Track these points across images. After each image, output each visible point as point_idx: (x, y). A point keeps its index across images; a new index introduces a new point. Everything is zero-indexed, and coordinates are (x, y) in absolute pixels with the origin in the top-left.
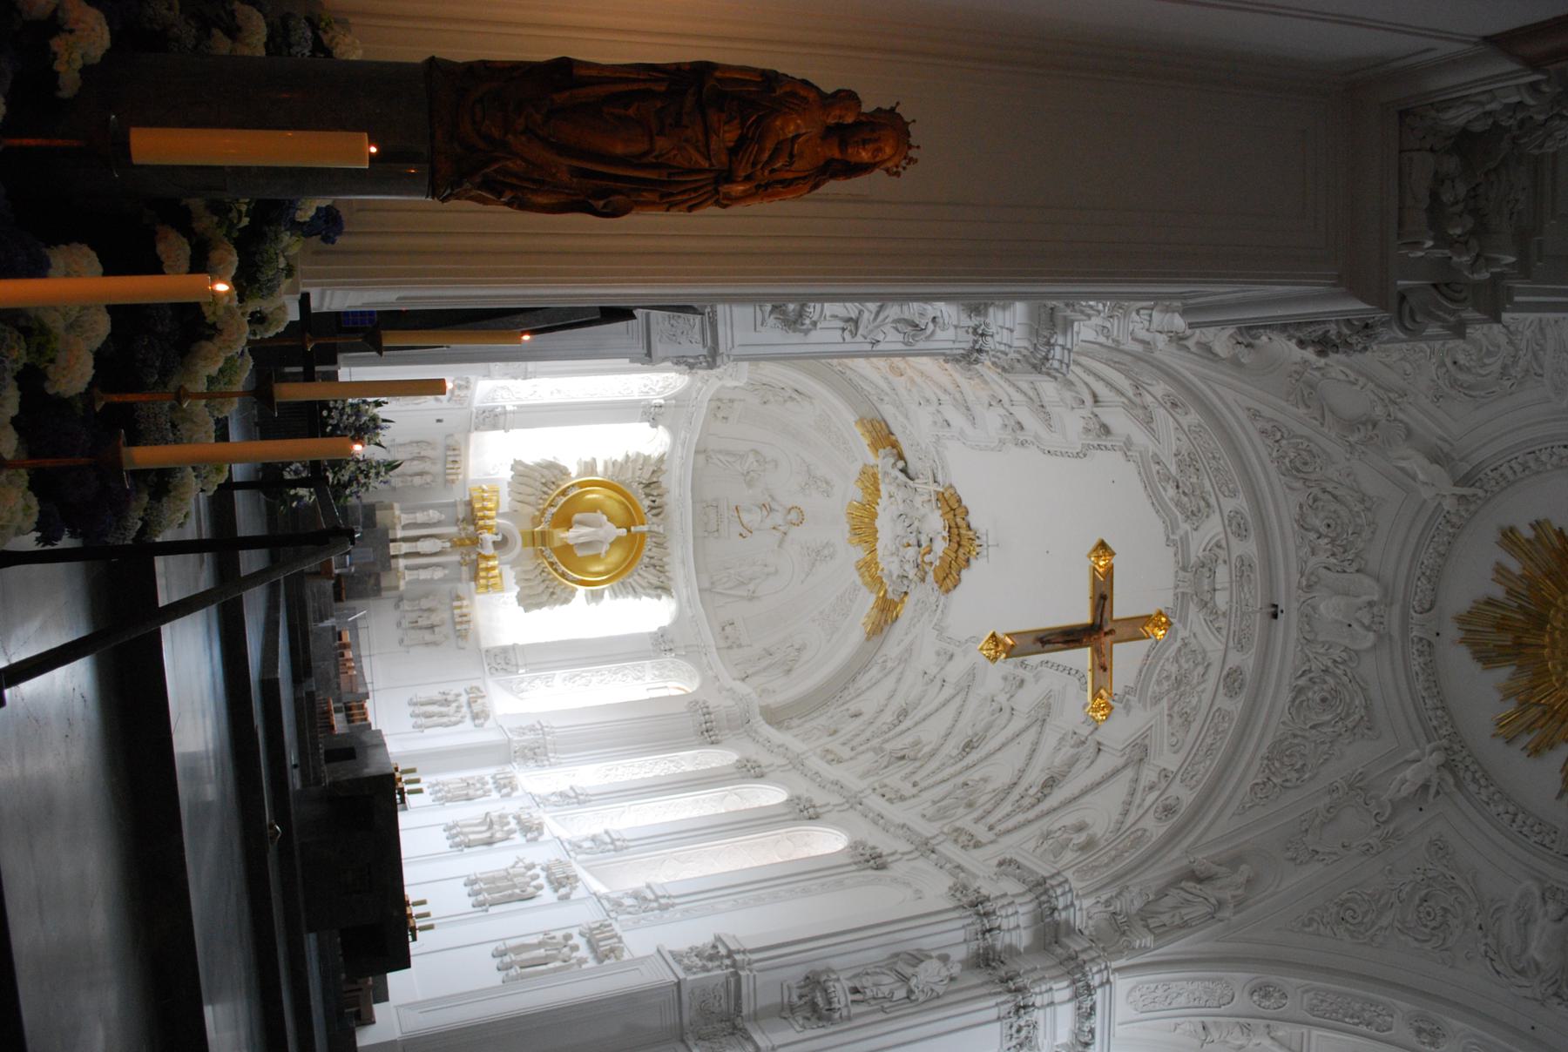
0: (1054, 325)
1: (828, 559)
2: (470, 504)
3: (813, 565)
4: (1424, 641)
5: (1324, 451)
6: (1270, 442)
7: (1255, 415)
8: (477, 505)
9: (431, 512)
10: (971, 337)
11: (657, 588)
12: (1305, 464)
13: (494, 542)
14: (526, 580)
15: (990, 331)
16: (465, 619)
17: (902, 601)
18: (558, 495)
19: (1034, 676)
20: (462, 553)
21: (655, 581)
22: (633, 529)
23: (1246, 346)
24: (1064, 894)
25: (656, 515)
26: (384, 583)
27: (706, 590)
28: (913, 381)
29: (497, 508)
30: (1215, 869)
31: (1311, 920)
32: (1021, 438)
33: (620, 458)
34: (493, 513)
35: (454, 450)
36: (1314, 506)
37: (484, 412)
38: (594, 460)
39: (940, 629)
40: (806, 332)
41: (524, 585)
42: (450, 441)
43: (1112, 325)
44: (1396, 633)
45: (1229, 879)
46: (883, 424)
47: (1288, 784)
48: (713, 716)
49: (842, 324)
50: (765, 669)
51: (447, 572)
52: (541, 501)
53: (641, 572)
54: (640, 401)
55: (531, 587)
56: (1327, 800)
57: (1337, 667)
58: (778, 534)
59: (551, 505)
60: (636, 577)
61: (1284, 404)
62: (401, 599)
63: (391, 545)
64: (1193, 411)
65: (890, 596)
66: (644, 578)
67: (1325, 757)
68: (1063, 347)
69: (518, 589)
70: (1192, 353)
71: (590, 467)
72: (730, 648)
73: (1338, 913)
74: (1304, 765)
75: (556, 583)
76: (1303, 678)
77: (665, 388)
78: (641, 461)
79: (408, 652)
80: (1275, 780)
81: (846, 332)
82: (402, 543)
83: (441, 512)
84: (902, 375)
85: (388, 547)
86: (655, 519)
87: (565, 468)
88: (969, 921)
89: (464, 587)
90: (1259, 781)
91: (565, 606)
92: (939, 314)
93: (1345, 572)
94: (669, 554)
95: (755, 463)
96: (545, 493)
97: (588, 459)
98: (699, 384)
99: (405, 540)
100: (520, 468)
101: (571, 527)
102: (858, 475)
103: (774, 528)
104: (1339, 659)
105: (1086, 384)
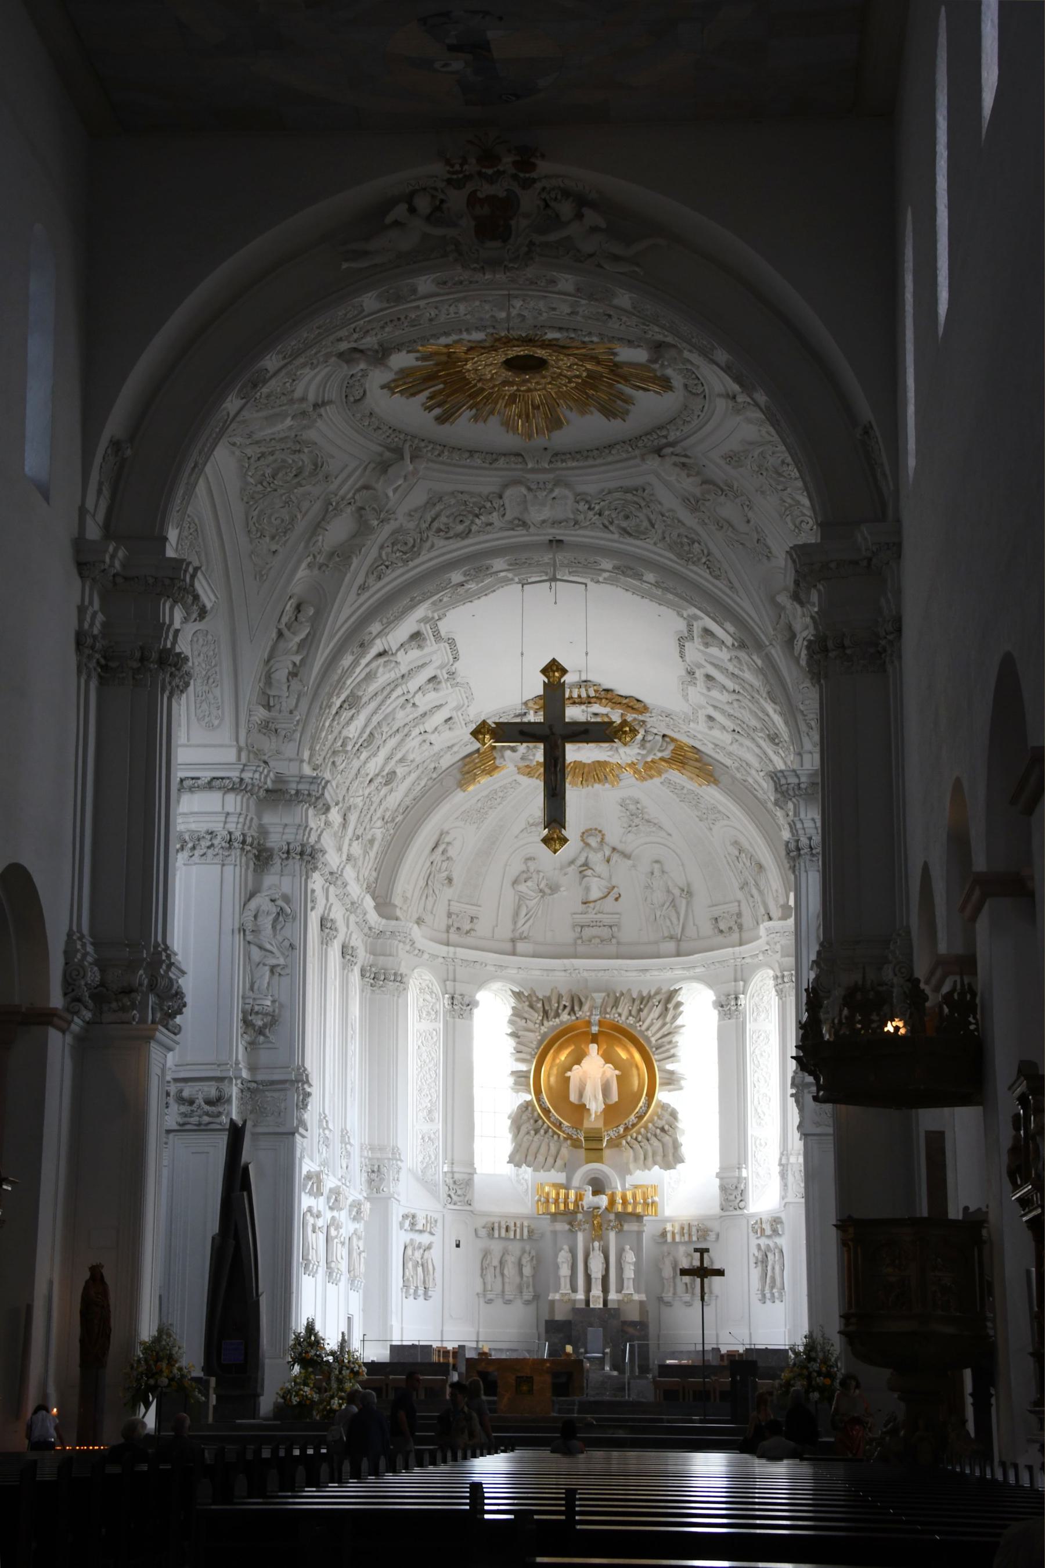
0: (281, 790)
1: (639, 806)
2: (554, 1216)
3: (648, 821)
4: (553, 460)
5: (392, 534)
6: (389, 571)
7: (363, 588)
8: (553, 1209)
9: (560, 1260)
10: (290, 861)
11: (666, 1009)
12: (406, 544)
13: (595, 1193)
14: (645, 1159)
15: (285, 848)
16: (685, 1231)
17: (673, 740)
18: (549, 1118)
19: (699, 668)
20: (607, 1229)
21: (656, 1012)
22: (595, 1029)
23: (299, 611)
24: (785, 777)
25: (581, 1004)
26: (634, 1316)
27: (678, 945)
28: (402, 760)
29: (557, 1186)
32: (446, 676)
33: (511, 1043)
34: (562, 1192)
35: (493, 1229)
36: (446, 530)
37: (449, 1196)
38: (513, 1073)
39: (688, 720)
40: (281, 1006)
41: (650, 1160)
42: (483, 1233)
43: (284, 729)
44: (551, 476)
46: (468, 760)
47: (706, 552)
48: (786, 973)
49: (276, 976)
50: (760, 892)
51: (628, 1247)
52: (556, 1137)
53: (644, 1028)
54: (446, 1023)
55: (654, 1154)
58: (615, 857)
59: (560, 1126)
60: (649, 1033)
61: (349, 575)
62: (660, 1299)
63: (592, 1306)
64: (369, 629)
65: (667, 754)
66: (652, 1024)
68: (298, 783)
69: (656, 1167)
70: (308, 654)
71: (520, 1078)
72: (740, 927)
74: (686, 536)
75: (650, 1125)
77: (432, 992)
78: (518, 1019)
79: (717, 1297)
81: (282, 973)
82: (592, 1293)
83: (561, 1249)
84: (394, 772)
85: (594, 1309)
86: (586, 1008)
87: (520, 1107)
88: (802, 864)
89: (649, 1228)
91: (680, 1116)
92: (267, 899)
94: (629, 990)
95: (529, 883)
96: (546, 1132)
97: (511, 1080)
98: (426, 956)
99: (588, 1289)
100: (517, 1158)
101: (585, 1105)
102: (534, 779)
103: (608, 861)
105: (367, 665)
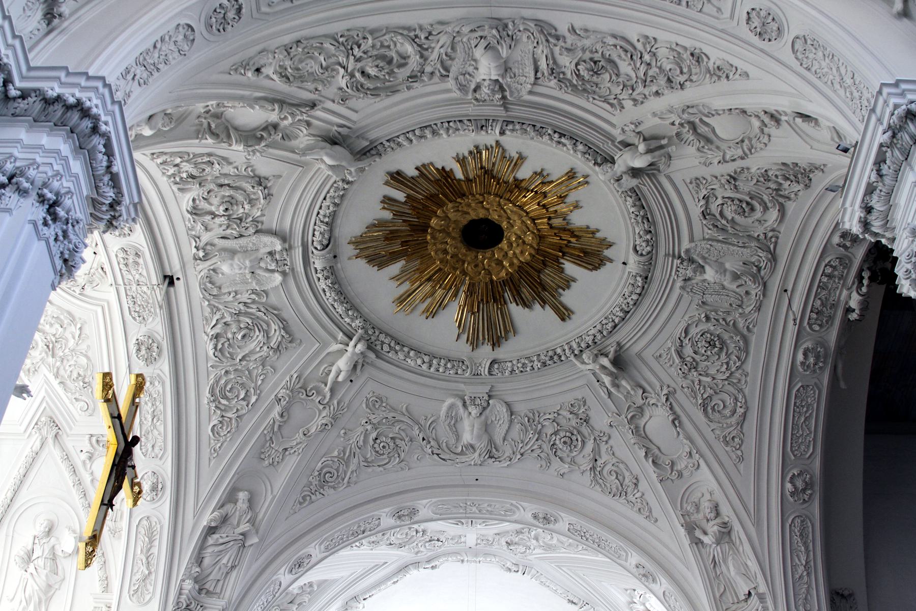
30: (223, 511)
31: (304, 498)
45: (237, 513)
56: (278, 409)
57: (248, 307)
67: (262, 377)
73: (320, 480)
76: (219, 326)
80: (230, 415)
90: (216, 422)
93: (241, 236)
104: (249, 301)
